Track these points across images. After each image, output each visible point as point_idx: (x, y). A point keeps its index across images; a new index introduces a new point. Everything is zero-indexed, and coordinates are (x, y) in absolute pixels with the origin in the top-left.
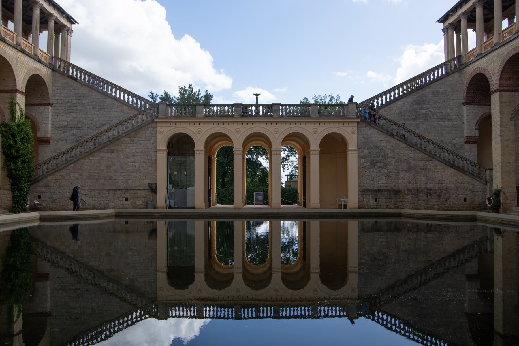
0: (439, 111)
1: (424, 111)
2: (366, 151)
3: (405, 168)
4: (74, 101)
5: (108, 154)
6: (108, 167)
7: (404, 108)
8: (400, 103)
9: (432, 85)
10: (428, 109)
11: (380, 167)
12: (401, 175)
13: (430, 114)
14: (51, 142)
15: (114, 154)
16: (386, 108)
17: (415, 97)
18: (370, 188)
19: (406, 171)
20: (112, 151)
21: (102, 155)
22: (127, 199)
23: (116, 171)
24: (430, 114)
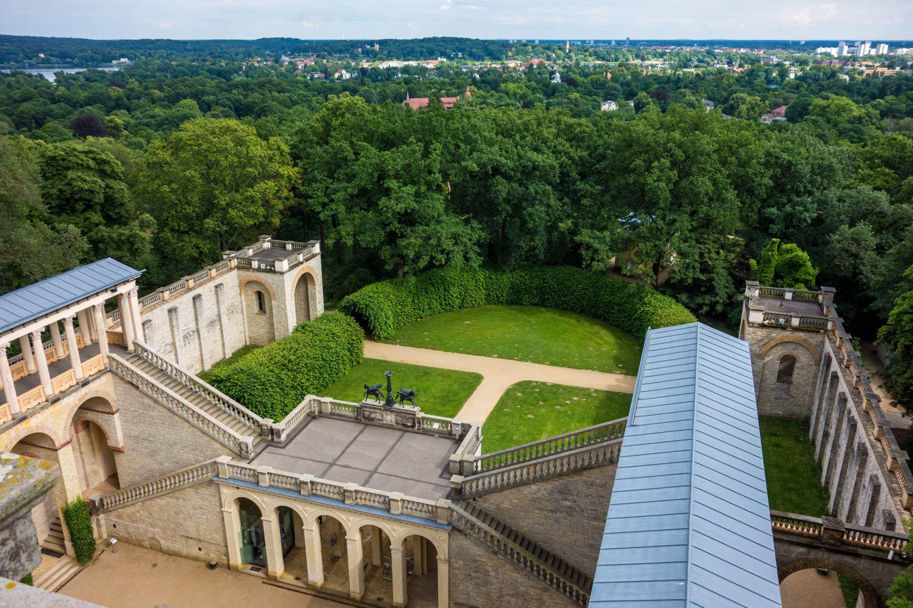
0: (592, 508)
1: (568, 504)
2: (461, 562)
3: (511, 592)
4: (141, 411)
5: (175, 501)
6: (177, 514)
7: (539, 495)
8: (534, 487)
9: (586, 473)
10: (575, 501)
11: (477, 584)
12: (506, 598)
13: (577, 508)
14: (126, 450)
15: (181, 502)
16: (514, 490)
17: (557, 483)
18: (464, 602)
19: (512, 596)
20: (178, 499)
21: (169, 500)
22: (200, 549)
23: (184, 519)
24: (577, 508)
